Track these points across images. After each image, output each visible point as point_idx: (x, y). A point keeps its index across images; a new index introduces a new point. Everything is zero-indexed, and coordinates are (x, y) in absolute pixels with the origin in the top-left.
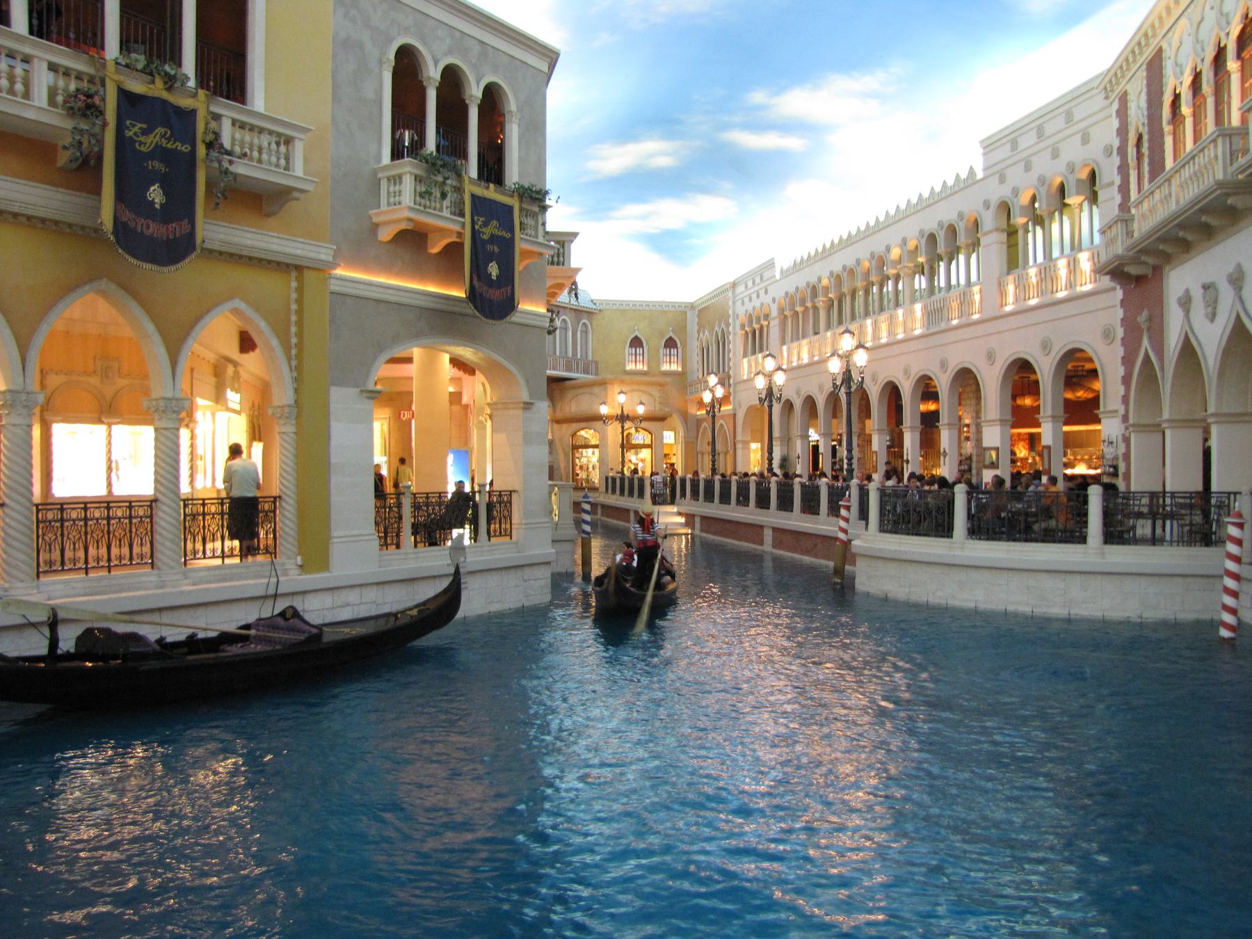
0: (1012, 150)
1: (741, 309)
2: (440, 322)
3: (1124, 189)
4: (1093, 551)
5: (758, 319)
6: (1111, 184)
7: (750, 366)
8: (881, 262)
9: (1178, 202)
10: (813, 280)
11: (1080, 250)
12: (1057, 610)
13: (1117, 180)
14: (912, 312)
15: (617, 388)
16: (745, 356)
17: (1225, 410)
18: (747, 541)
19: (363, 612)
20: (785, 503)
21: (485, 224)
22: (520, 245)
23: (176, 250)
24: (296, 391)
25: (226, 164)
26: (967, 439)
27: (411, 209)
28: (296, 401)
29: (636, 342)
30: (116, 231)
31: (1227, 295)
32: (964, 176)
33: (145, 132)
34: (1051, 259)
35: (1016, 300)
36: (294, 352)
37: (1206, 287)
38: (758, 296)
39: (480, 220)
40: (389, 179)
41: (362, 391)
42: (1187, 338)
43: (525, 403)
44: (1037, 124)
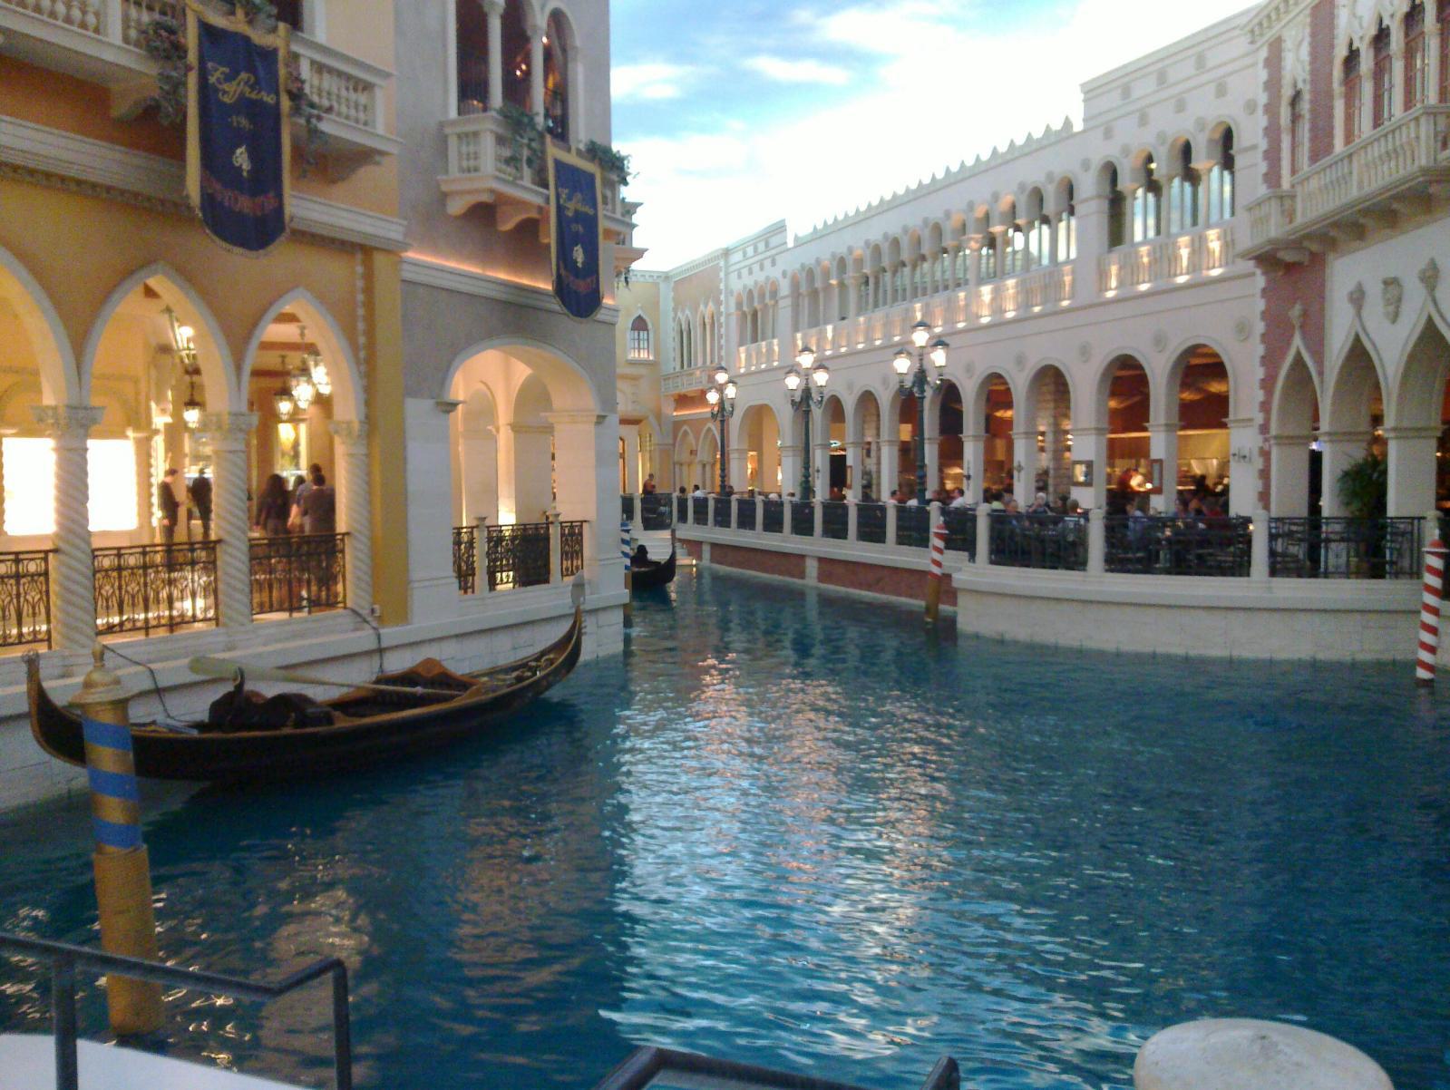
0: (1124, 99)
1: (738, 282)
2: (513, 319)
3: (1272, 156)
4: (1258, 584)
5: (762, 296)
6: (1254, 147)
7: (749, 357)
8: (937, 230)
9: (1360, 186)
10: (842, 250)
11: (1208, 226)
12: (1216, 650)
13: (1263, 145)
14: (979, 295)
16: (741, 344)
17: (1405, 424)
18: (781, 573)
20: (836, 528)
21: (569, 198)
22: (603, 224)
23: (260, 230)
24: (368, 403)
25: (314, 121)
26: (1042, 449)
27: (497, 178)
28: (367, 417)
30: (203, 208)
31: (1415, 296)
33: (229, 78)
34: (1169, 235)
35: (1121, 284)
36: (362, 354)
37: (1387, 283)
38: (762, 268)
39: (564, 192)
40: (459, 136)
41: (438, 403)
42: (1357, 339)
43: (599, 417)
44: (1158, 67)
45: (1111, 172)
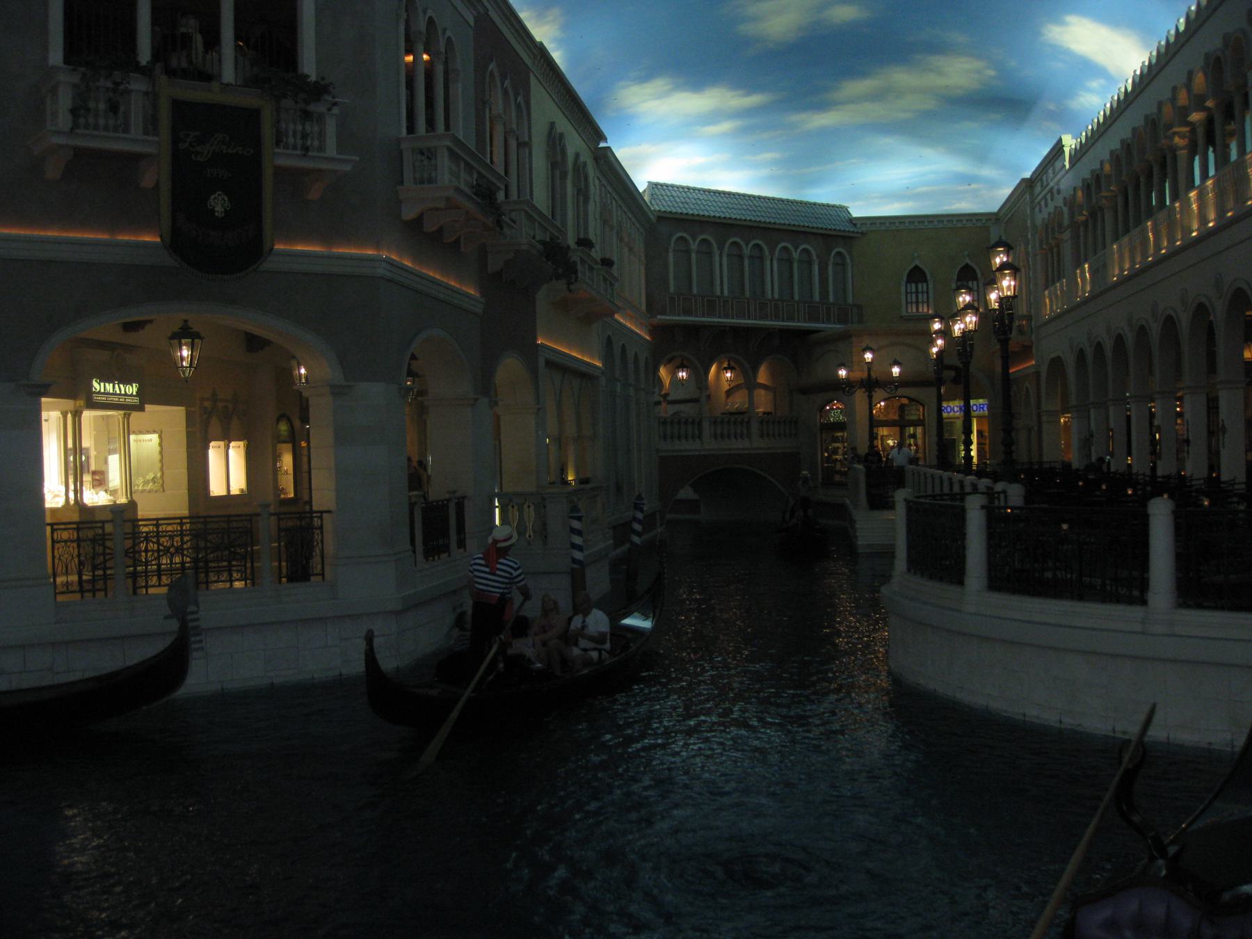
1: (1041, 217)
5: (1053, 229)
15: (866, 341)
19: (28, 682)
29: (917, 275)
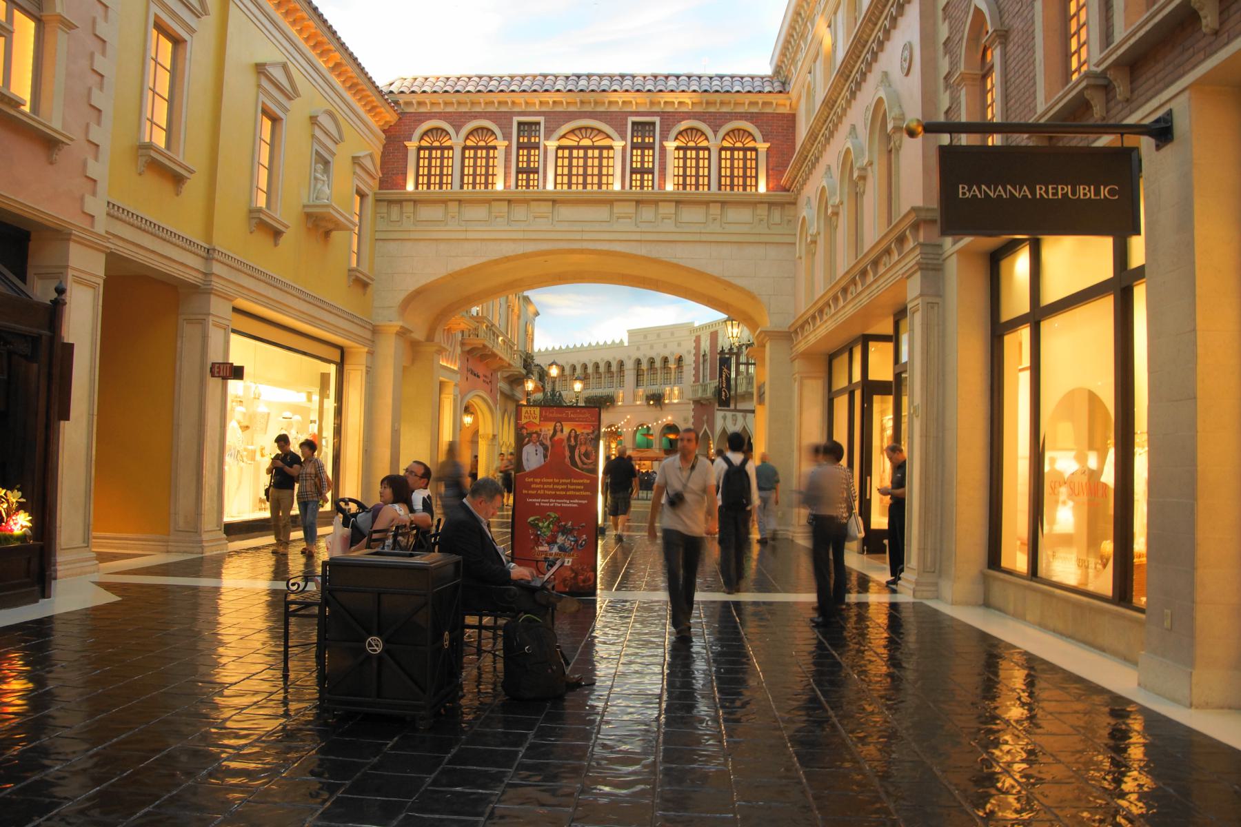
3: (697, 369)
32: (617, 341)
44: (658, 332)
45: (638, 362)
